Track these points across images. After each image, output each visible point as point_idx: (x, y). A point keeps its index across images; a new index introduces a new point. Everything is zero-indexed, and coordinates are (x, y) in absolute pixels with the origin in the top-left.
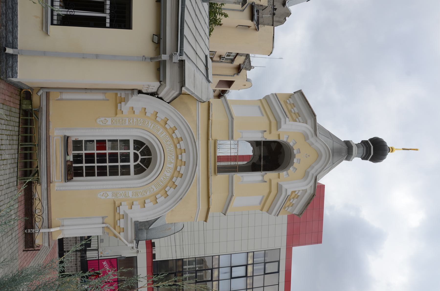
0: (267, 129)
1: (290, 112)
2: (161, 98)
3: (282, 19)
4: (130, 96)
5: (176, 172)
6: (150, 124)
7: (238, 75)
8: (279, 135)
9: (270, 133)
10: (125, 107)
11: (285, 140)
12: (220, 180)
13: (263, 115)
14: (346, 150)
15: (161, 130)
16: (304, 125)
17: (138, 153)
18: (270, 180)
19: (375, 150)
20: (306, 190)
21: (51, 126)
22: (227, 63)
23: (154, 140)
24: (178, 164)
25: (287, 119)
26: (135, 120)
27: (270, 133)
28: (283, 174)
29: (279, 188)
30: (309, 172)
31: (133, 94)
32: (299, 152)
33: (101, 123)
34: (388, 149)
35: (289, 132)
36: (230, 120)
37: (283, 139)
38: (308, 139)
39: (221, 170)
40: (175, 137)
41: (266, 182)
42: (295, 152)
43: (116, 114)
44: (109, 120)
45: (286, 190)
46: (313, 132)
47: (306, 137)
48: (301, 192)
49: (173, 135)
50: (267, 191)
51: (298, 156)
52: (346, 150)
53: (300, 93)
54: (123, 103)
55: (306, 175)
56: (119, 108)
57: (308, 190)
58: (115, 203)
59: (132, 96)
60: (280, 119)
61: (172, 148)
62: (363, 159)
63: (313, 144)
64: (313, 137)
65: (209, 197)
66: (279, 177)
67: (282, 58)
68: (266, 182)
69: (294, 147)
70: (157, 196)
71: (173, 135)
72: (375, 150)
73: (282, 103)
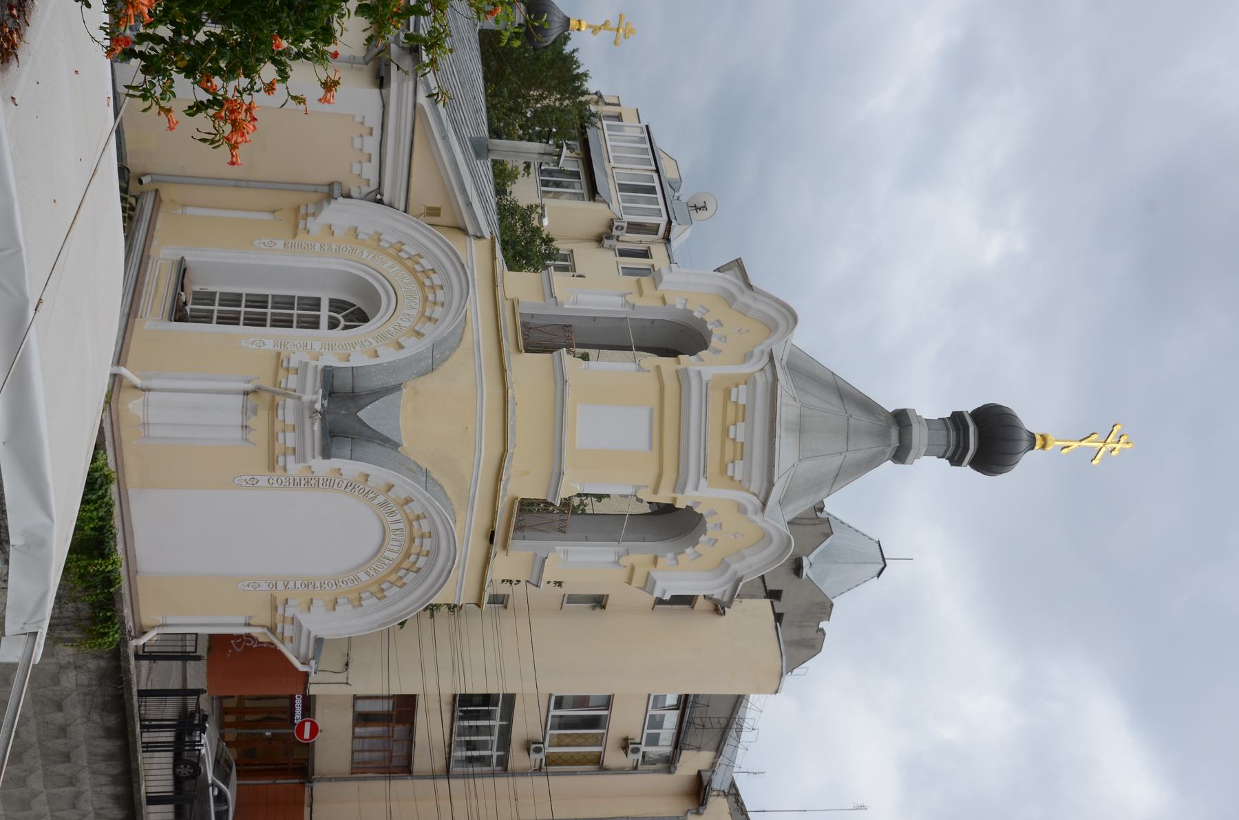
2: (391, 206)
3: (810, 633)
4: (325, 205)
6: (365, 254)
7: (698, 813)
9: (641, 293)
10: (314, 225)
11: (679, 306)
12: (529, 370)
14: (897, 434)
15: (390, 263)
17: (339, 316)
18: (658, 368)
19: (988, 439)
20: (753, 374)
21: (155, 243)
22: (655, 771)
23: (370, 274)
26: (334, 247)
27: (641, 293)
29: (682, 378)
31: (330, 197)
32: (720, 324)
33: (262, 246)
34: (1025, 436)
39: (532, 347)
42: (710, 327)
43: (295, 235)
44: (280, 244)
45: (699, 372)
46: (741, 283)
48: (742, 388)
50: (654, 387)
52: (897, 434)
54: (310, 219)
56: (301, 225)
57: (757, 375)
58: (279, 355)
59: (329, 203)
61: (415, 287)
62: (956, 461)
63: (749, 307)
64: (743, 292)
65: (503, 371)
66: (679, 363)
67: (862, 807)
69: (705, 318)
72: (988, 439)
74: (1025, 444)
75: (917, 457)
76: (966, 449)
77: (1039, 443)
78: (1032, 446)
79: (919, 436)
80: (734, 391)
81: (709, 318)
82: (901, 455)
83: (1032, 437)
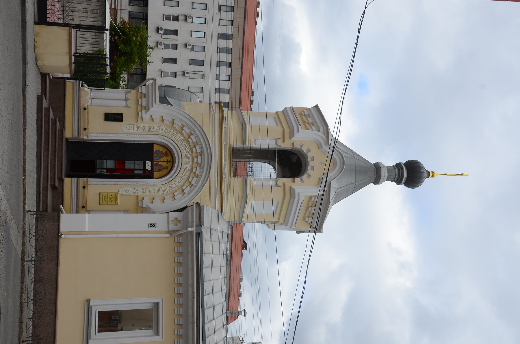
0: (280, 136)
1: (304, 122)
5: (192, 173)
8: (293, 144)
9: (284, 141)
11: (298, 147)
13: (277, 125)
16: (318, 133)
24: (194, 166)
25: (300, 127)
27: (284, 141)
28: (297, 180)
32: (313, 159)
35: (303, 139)
37: (297, 146)
40: (191, 141)
41: (280, 187)
42: (309, 159)
51: (311, 163)
53: (317, 106)
60: (293, 126)
68: (280, 187)
70: (175, 194)
71: (190, 140)
73: (298, 117)
74: (426, 175)
75: (383, 181)
76: (403, 176)
77: (431, 174)
78: (428, 176)
79: (384, 173)
80: (313, 198)
81: (309, 155)
82: (377, 181)
83: (428, 172)
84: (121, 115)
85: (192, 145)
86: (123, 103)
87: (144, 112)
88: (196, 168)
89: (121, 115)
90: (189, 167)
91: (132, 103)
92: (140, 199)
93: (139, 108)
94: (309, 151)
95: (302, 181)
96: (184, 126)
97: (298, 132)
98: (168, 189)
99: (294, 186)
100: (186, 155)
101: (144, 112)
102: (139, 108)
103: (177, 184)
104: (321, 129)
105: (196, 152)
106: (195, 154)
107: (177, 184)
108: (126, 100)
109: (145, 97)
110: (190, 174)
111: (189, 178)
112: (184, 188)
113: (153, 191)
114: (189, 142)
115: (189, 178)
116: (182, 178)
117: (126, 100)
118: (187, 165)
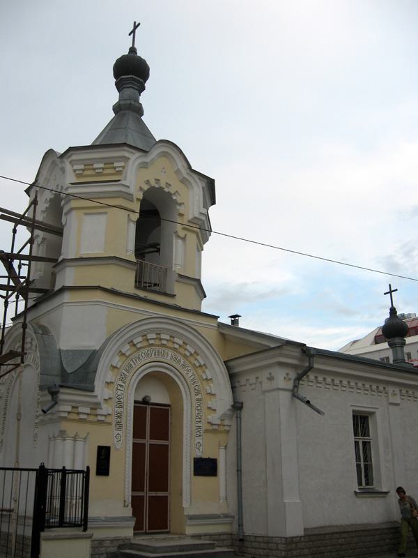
13: (106, 213)
30: (184, 178)
32: (157, 181)
36: (114, 261)
38: (147, 163)
45: (201, 213)
47: (144, 166)
49: (138, 346)
51: (163, 185)
55: (184, 181)
84: (100, 448)
85: (145, 344)
86: (80, 444)
87: (99, 412)
88: (174, 343)
89: (100, 448)
90: (170, 353)
91: (82, 429)
92: (210, 427)
93: (92, 418)
94: (148, 182)
95: (180, 204)
96: (121, 351)
97: (128, 187)
98: (197, 388)
99: (191, 217)
100: (155, 355)
101: (99, 412)
102: (92, 418)
103: (190, 374)
104: (126, 154)
105: (168, 340)
106: (170, 344)
107: (190, 374)
108: (75, 439)
109: (77, 407)
110: (181, 354)
111: (185, 356)
112: (198, 365)
113: (199, 408)
114: (141, 348)
115: (185, 356)
116: (184, 366)
117: (75, 439)
118: (169, 356)
